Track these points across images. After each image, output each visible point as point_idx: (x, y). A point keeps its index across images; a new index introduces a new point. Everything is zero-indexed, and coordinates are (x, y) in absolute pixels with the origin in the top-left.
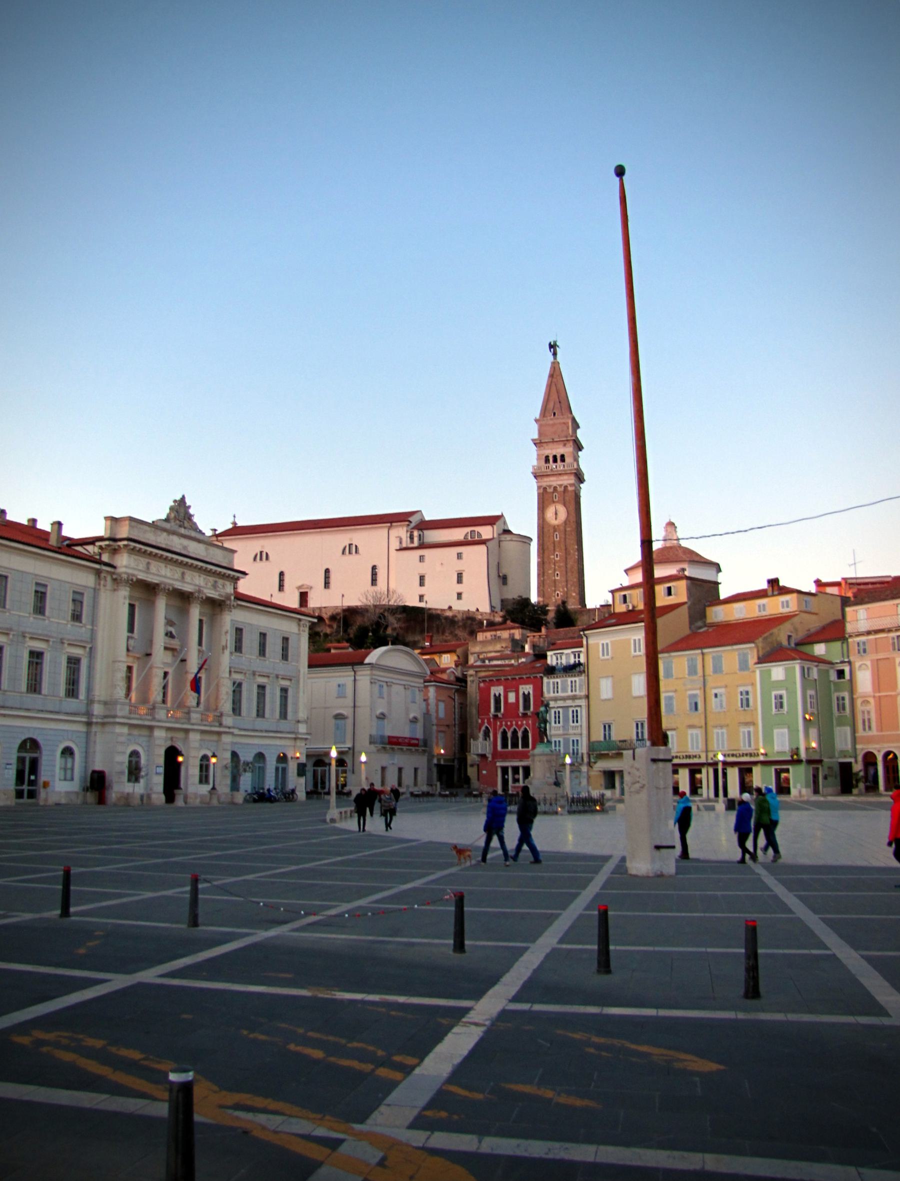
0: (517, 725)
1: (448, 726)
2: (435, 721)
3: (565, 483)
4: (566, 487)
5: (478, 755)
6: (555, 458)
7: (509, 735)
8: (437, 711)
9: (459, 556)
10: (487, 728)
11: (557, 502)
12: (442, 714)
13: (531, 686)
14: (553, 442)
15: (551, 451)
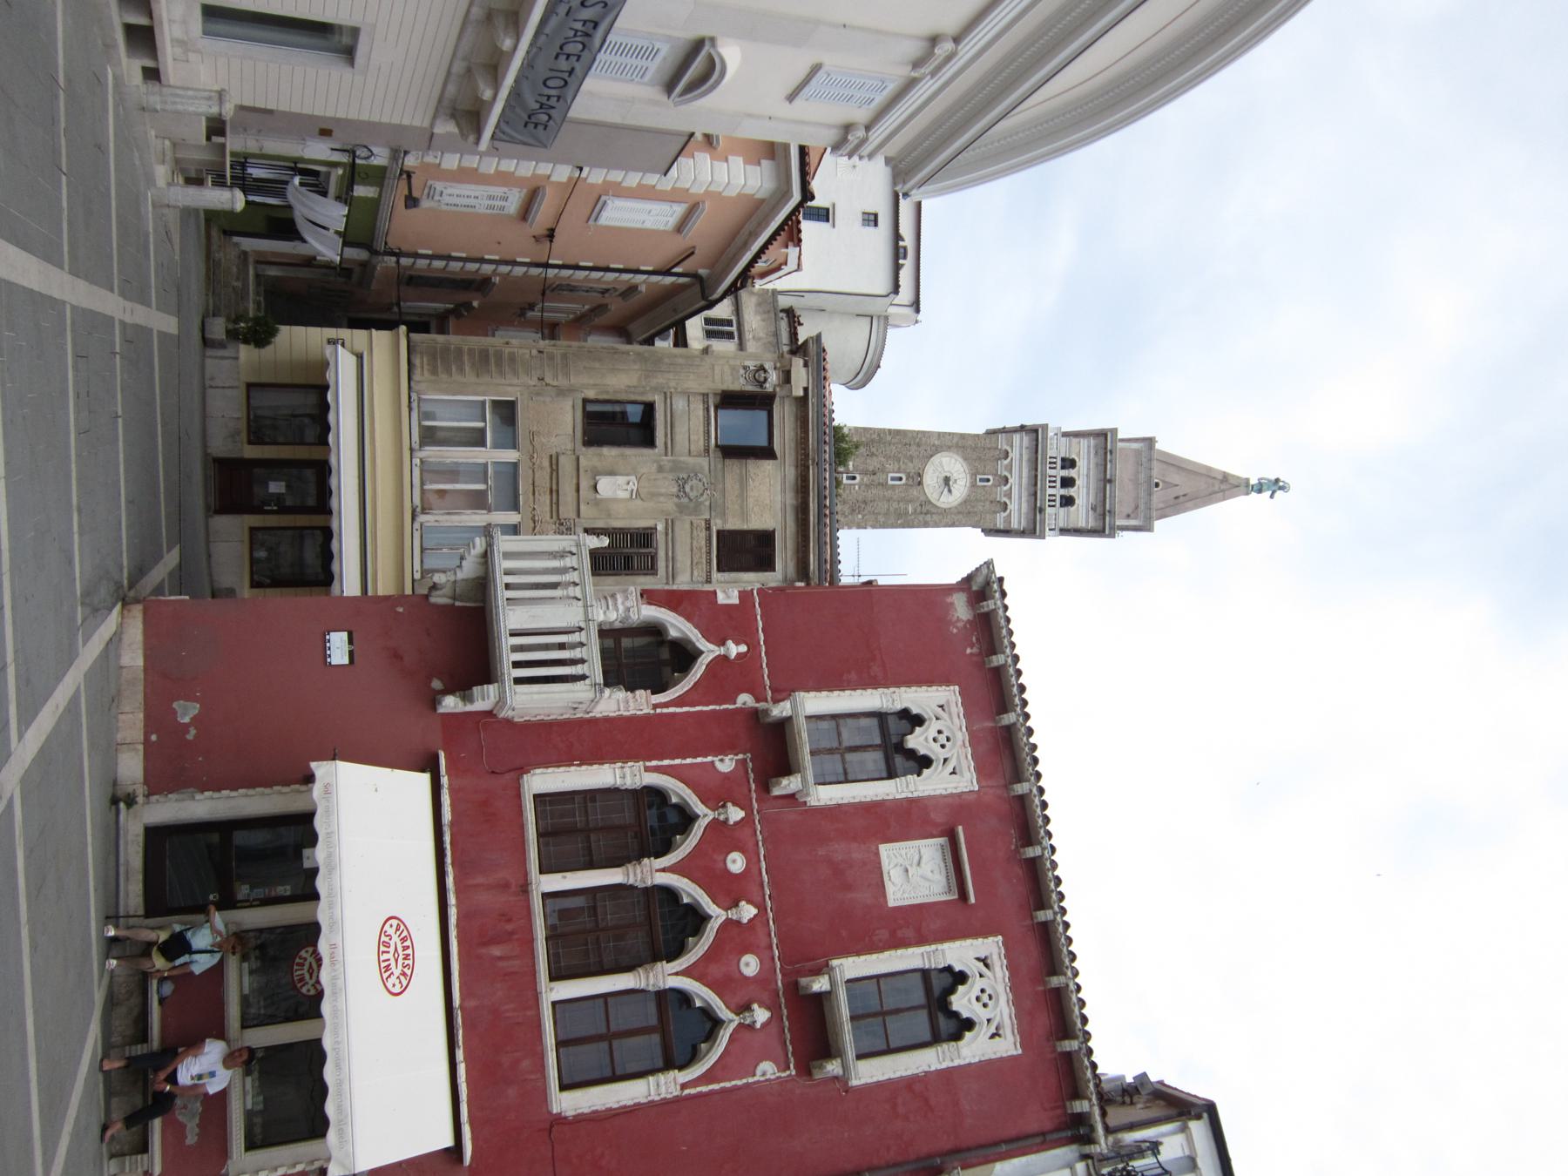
0: (736, 938)
1: (551, 235)
2: (595, 177)
3: (1013, 506)
4: (1005, 507)
5: (482, 585)
6: (1067, 482)
7: (654, 872)
8: (645, 194)
9: (872, 219)
10: (684, 656)
11: (973, 485)
12: (620, 214)
13: (1008, 1046)
14: (1106, 481)
15: (1084, 473)
